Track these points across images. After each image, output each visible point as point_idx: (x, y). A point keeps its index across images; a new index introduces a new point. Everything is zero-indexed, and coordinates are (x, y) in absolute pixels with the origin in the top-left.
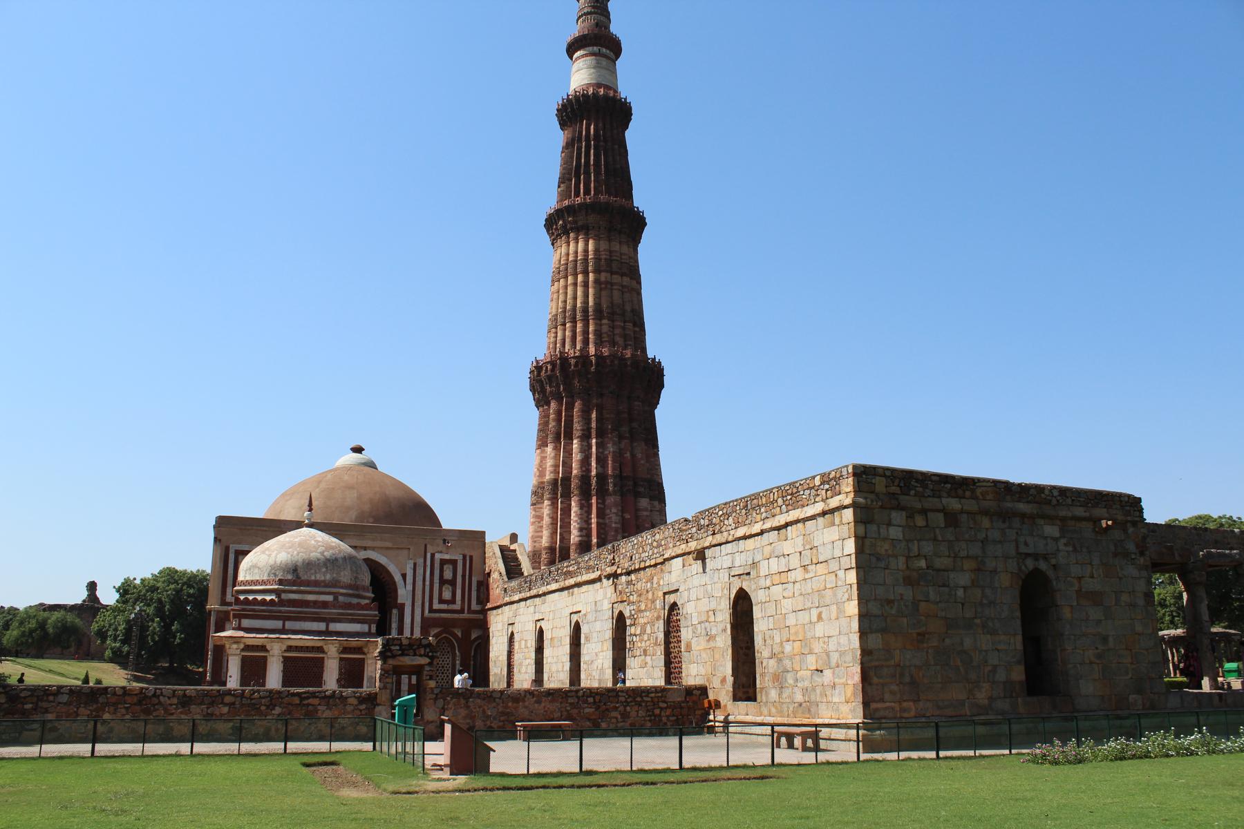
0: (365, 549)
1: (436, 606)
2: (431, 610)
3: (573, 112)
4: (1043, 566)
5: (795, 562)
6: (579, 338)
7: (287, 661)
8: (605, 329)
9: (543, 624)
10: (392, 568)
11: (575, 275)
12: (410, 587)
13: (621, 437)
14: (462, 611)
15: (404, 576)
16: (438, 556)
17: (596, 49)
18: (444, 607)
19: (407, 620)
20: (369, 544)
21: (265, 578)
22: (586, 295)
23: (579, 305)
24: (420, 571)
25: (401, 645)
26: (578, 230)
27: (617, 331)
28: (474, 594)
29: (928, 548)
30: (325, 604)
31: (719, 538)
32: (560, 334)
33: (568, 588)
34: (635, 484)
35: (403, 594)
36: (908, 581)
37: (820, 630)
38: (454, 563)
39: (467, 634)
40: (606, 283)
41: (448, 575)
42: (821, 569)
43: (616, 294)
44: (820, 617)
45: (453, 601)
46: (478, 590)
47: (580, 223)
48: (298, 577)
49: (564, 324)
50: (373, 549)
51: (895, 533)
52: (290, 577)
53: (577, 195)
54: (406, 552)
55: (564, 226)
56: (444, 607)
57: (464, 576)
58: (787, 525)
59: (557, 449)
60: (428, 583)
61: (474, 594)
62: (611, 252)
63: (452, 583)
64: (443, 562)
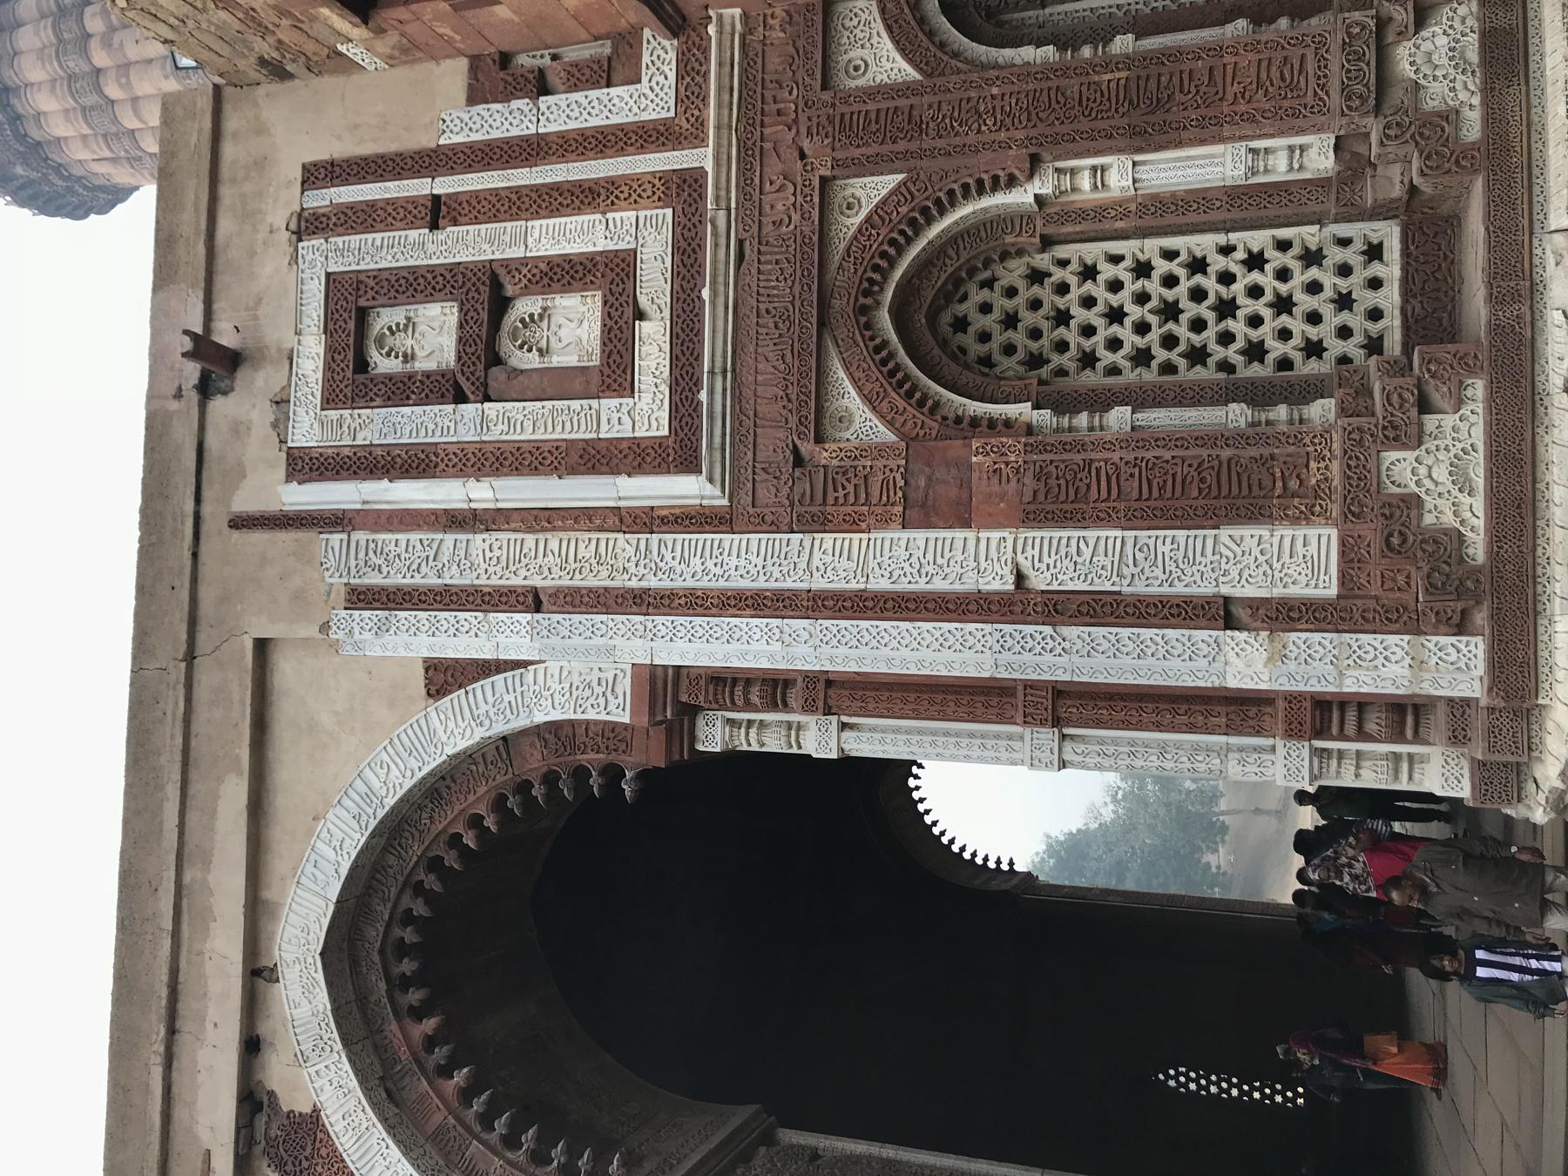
1: (646, 412)
2: (677, 453)
10: (392, 777)
14: (682, 190)
15: (445, 677)
16: (308, 430)
18: (653, 343)
24: (405, 559)
28: (565, 112)
38: (352, 307)
39: (876, 127)
45: (612, 275)
46: (541, 86)
54: (286, 670)
56: (653, 343)
57: (437, 213)
60: (481, 493)
61: (565, 112)
62: (43, 16)
63: (487, 296)
64: (353, 377)
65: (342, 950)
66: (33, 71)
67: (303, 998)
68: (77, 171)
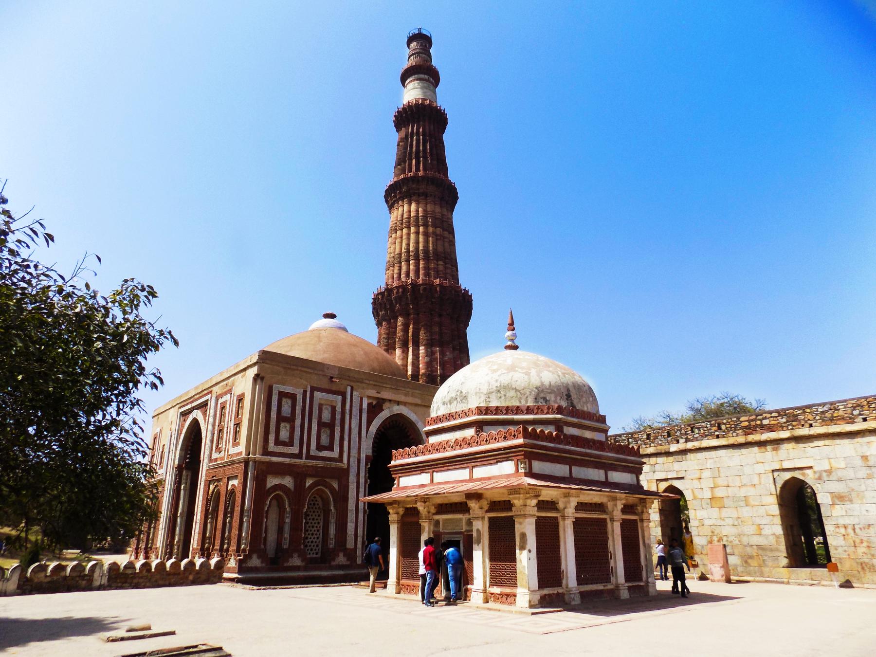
0: (398, 403)
3: (406, 117)
6: (421, 272)
7: (578, 524)
8: (441, 268)
9: (677, 484)
11: (417, 226)
13: (454, 349)
20: (402, 398)
21: (531, 403)
22: (426, 242)
23: (421, 248)
27: (449, 271)
33: (761, 444)
40: (441, 235)
43: (446, 244)
47: (421, 191)
48: (573, 406)
49: (408, 261)
50: (405, 404)
52: (564, 404)
53: (418, 169)
55: (408, 191)
59: (405, 352)
65: (400, 416)
67: (397, 409)
68: (400, 202)
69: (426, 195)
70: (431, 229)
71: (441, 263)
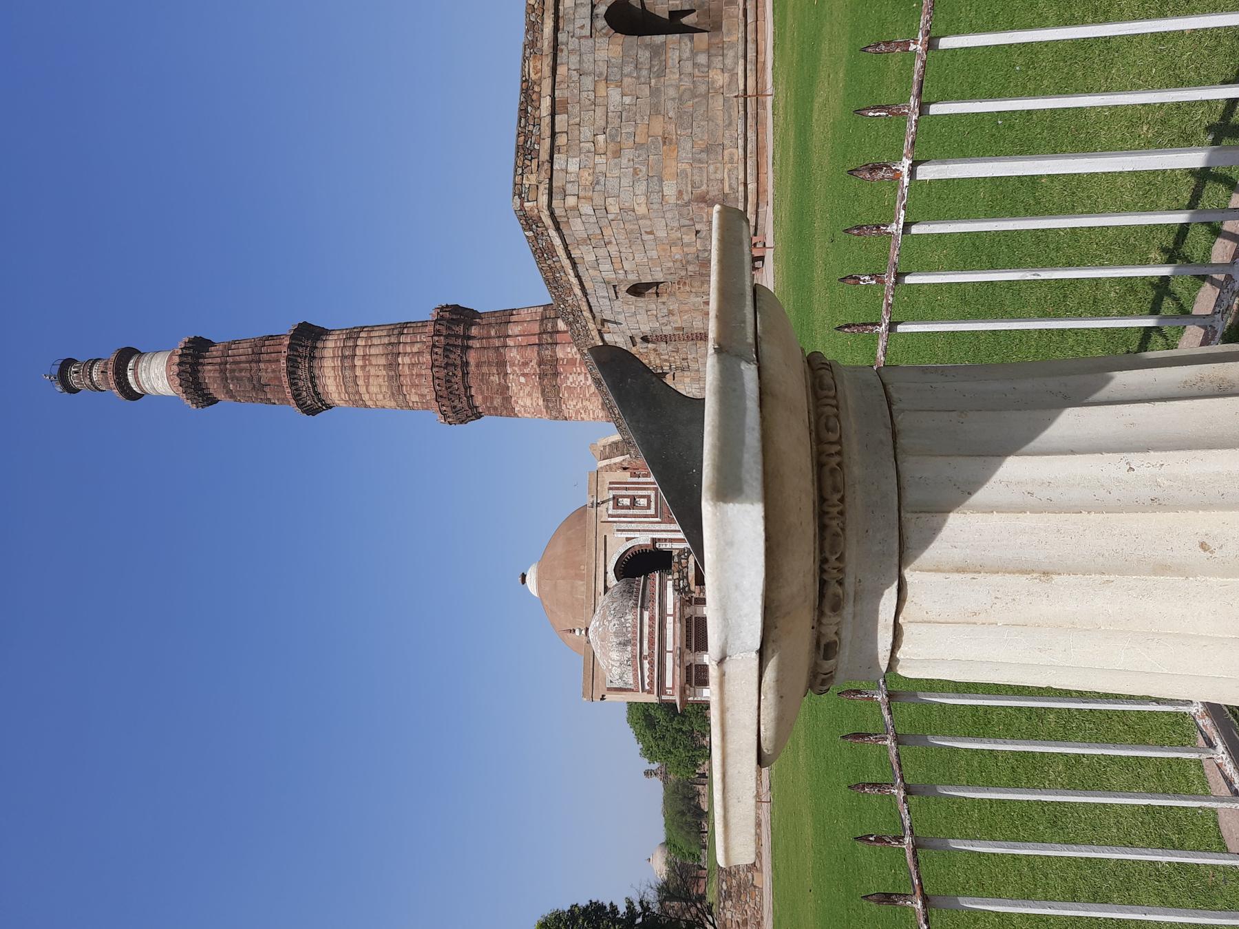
0: (606, 573)
1: (652, 511)
4: (602, 10)
5: (602, 252)
8: (407, 360)
12: (637, 535)
14: (656, 489)
17: (130, 373)
19: (664, 535)
24: (624, 526)
25: (679, 579)
26: (314, 386)
28: (641, 480)
29: (586, 132)
30: (652, 618)
31: (585, 307)
32: (415, 398)
34: (545, 332)
35: (643, 539)
36: (618, 154)
37: (661, 234)
41: (627, 502)
42: (607, 232)
43: (373, 351)
44: (651, 233)
45: (648, 497)
51: (573, 167)
52: (629, 648)
57: (626, 489)
58: (569, 257)
61: (641, 480)
66: (328, 372)
69: (313, 378)
70: (359, 372)
71: (400, 360)
